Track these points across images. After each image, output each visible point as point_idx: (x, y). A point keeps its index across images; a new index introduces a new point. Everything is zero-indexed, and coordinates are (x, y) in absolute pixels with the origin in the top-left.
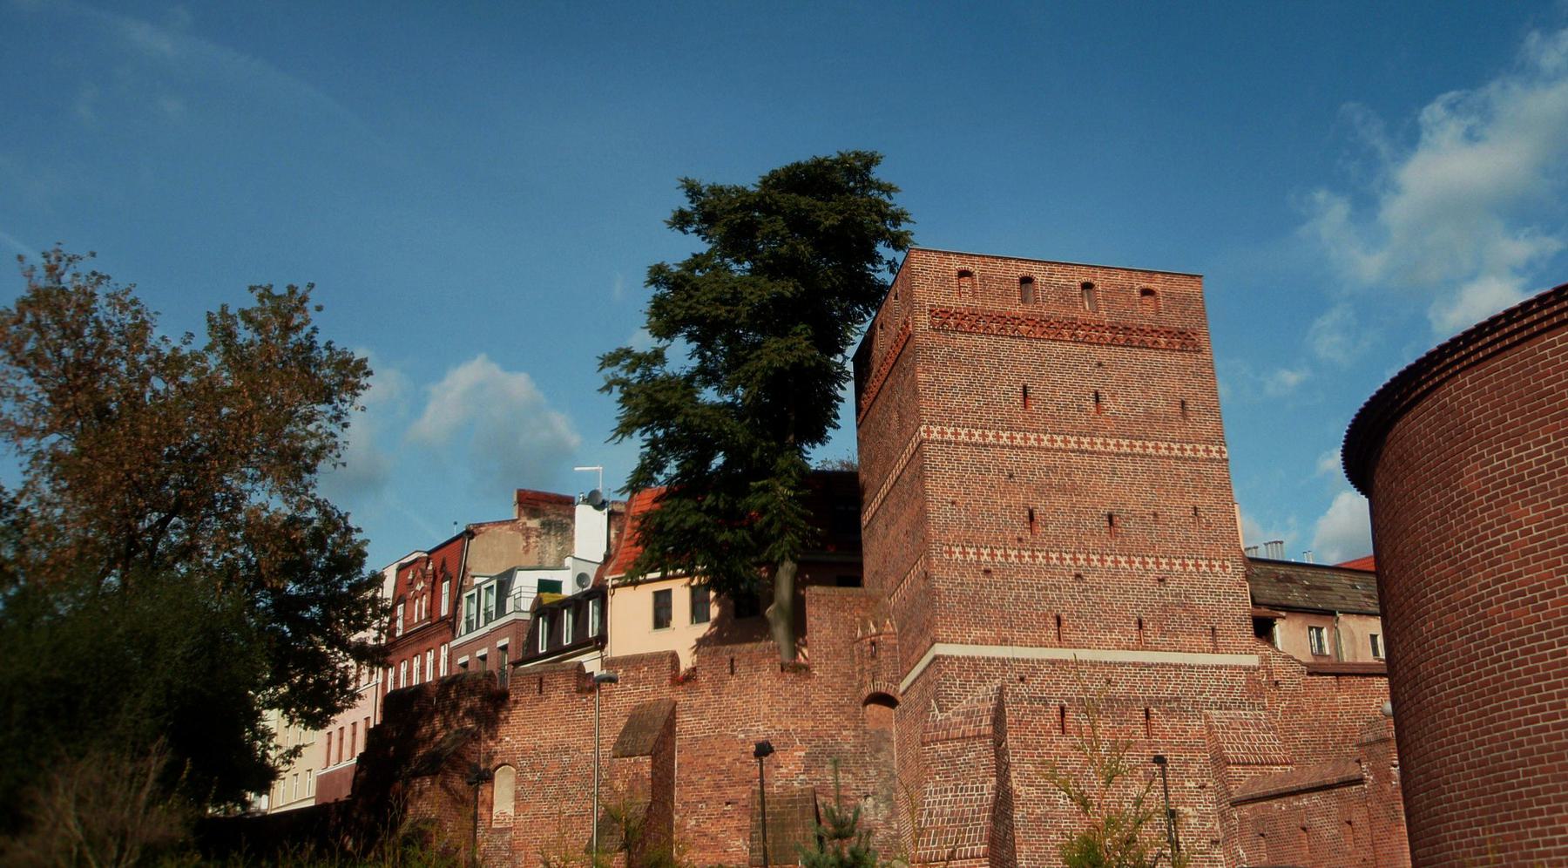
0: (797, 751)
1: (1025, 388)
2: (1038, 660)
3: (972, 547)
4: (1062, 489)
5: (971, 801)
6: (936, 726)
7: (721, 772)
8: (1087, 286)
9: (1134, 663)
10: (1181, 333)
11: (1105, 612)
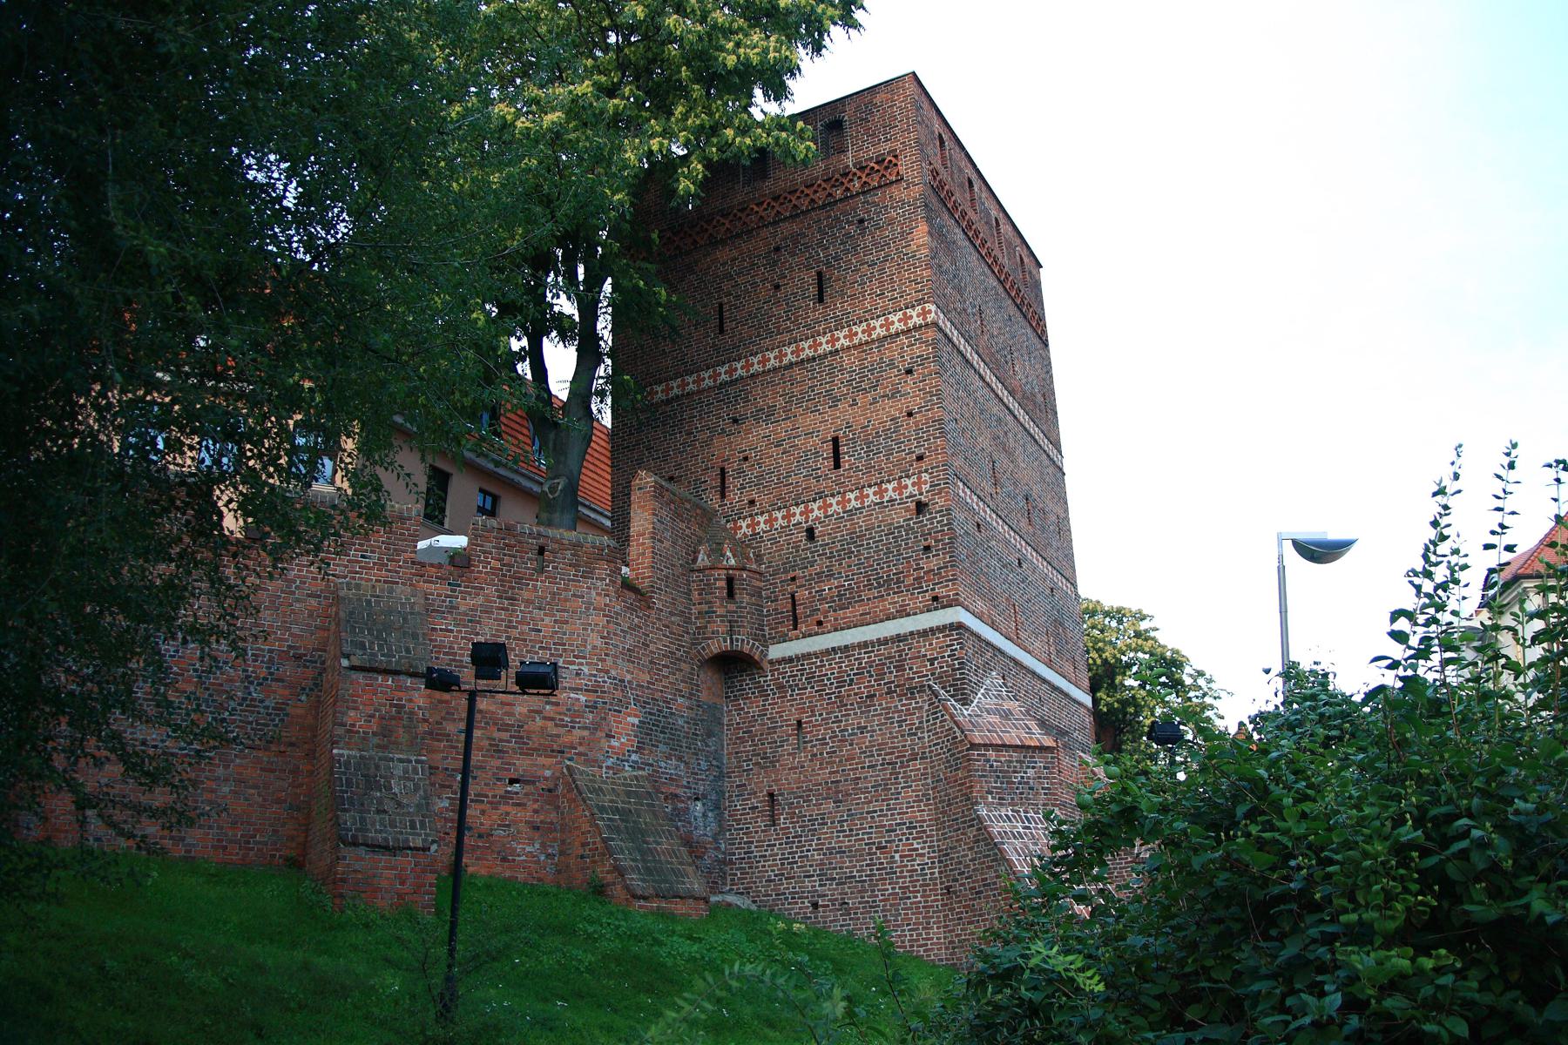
7: (505, 728)
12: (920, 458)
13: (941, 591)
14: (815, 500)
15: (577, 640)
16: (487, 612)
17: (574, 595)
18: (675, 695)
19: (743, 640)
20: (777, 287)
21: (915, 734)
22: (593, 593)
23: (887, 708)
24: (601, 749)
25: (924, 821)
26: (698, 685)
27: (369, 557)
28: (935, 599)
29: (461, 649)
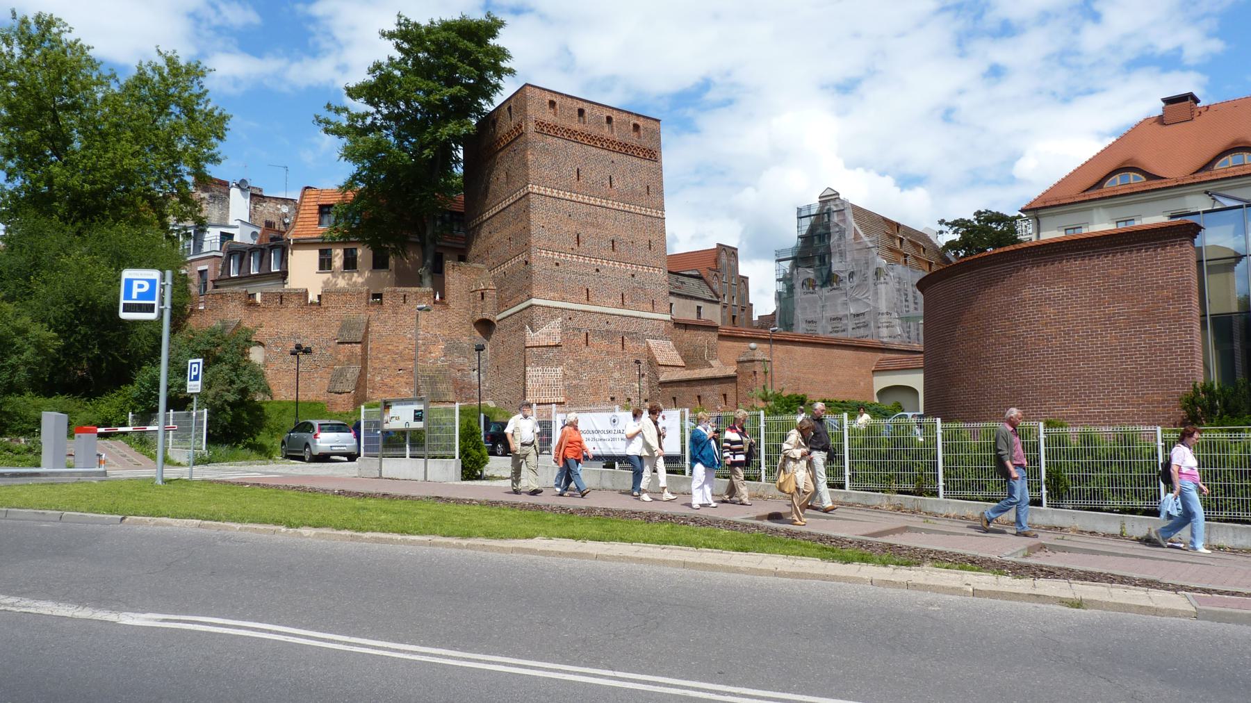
4: (592, 225)
7: (397, 354)
13: (529, 293)
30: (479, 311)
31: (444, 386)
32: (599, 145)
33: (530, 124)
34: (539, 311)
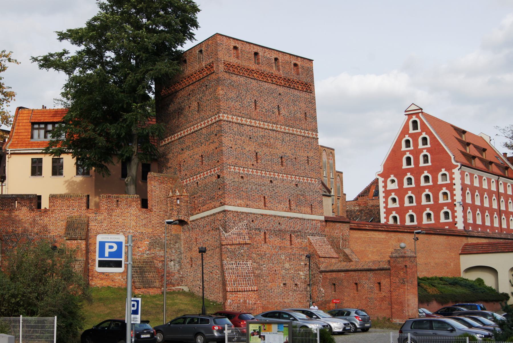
0: (145, 241)
1: (255, 100)
2: (258, 214)
3: (237, 167)
4: (266, 145)
5: (244, 269)
6: (226, 238)
8: (276, 59)
9: (288, 217)
10: (306, 84)
11: (279, 196)
12: (218, 162)
13: (222, 201)
14: (198, 174)
15: (128, 224)
16: (105, 219)
17: (127, 212)
18: (162, 234)
19: (181, 216)
20: (189, 107)
21: (217, 241)
22: (132, 211)
23: (212, 234)
24: (136, 251)
25: (219, 265)
26: (171, 230)
27: (75, 209)
28: (221, 203)
29: (99, 230)
30: (175, 213)
31: (151, 275)
32: (270, 81)
33: (220, 66)
34: (230, 216)
